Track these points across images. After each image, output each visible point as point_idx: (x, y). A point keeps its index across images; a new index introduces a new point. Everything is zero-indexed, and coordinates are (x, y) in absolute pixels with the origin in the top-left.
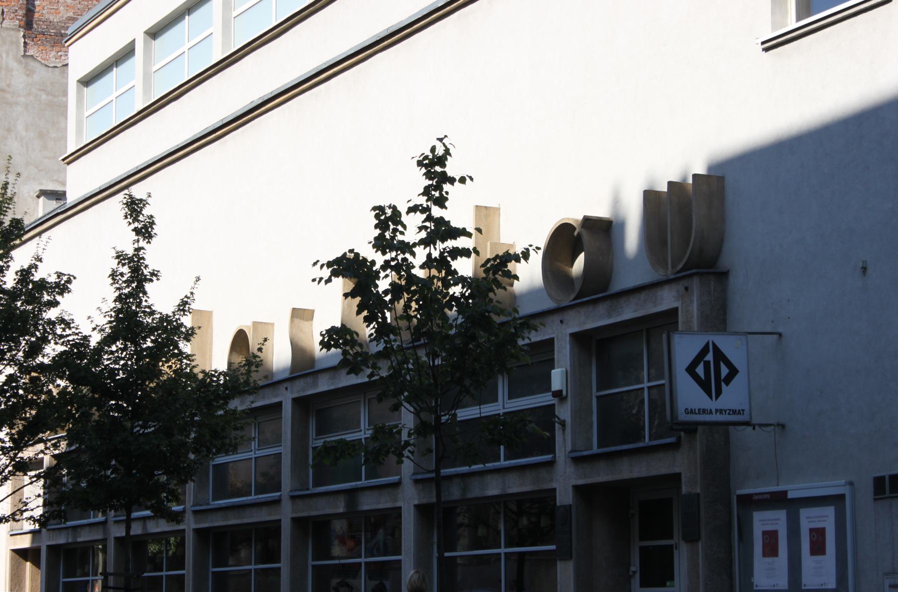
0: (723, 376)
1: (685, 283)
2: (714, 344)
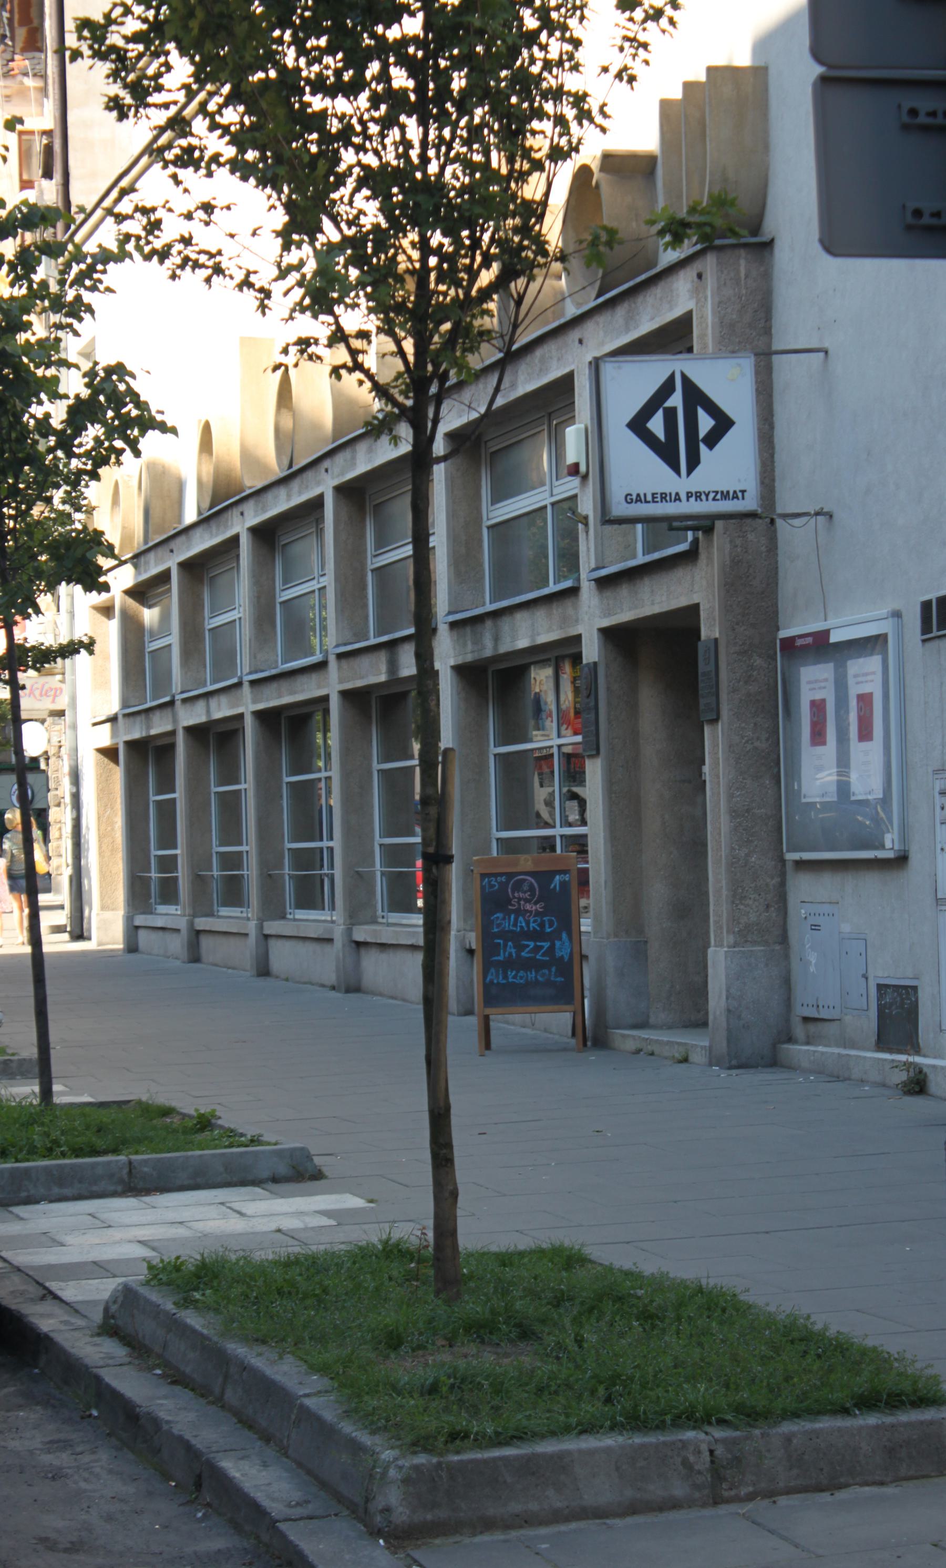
0: (702, 434)
1: (697, 266)
2: (684, 377)
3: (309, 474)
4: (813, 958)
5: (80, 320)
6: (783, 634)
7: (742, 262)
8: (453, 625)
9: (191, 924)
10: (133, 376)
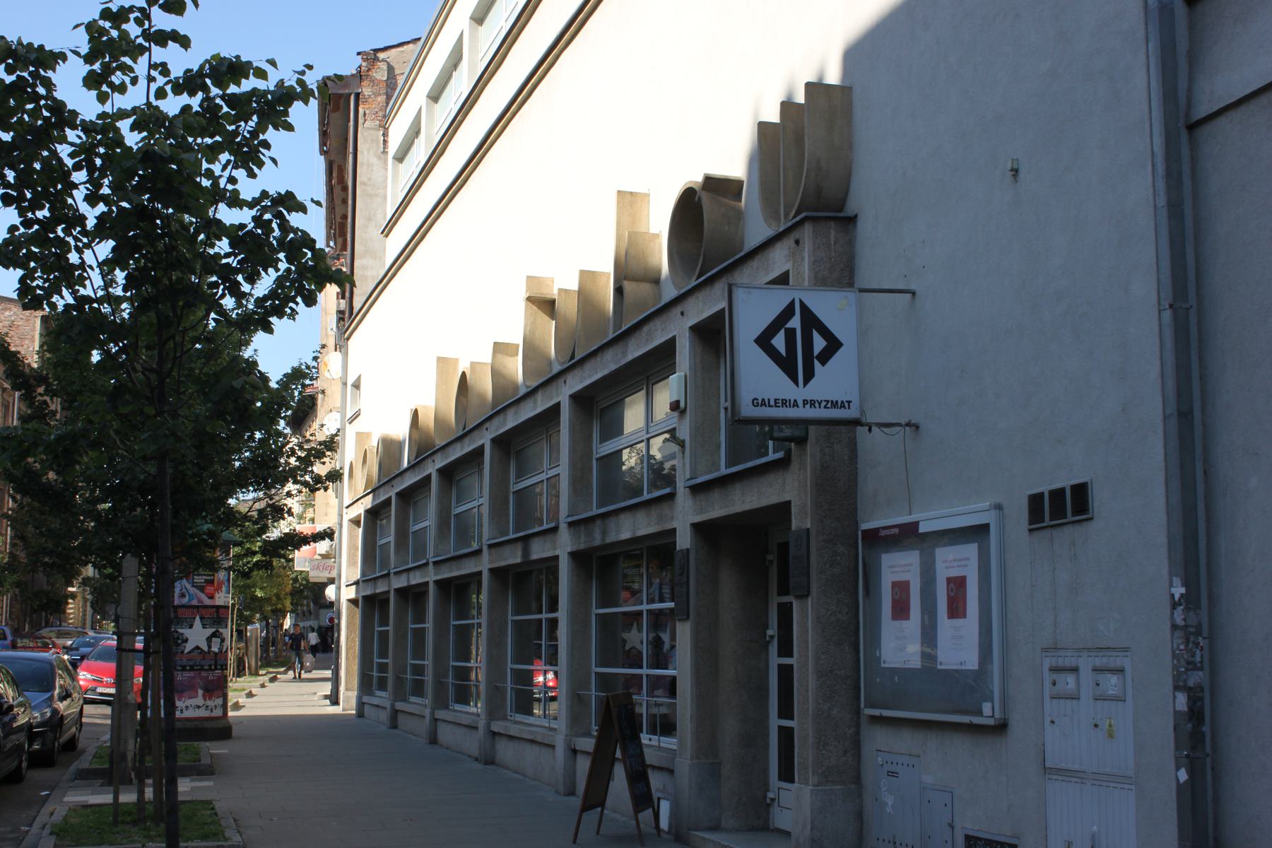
1: (795, 235)
2: (802, 303)
3: (476, 433)
4: (890, 800)
5: (260, 164)
6: (865, 526)
7: (832, 232)
8: (571, 524)
9: (393, 706)
10: (302, 208)
